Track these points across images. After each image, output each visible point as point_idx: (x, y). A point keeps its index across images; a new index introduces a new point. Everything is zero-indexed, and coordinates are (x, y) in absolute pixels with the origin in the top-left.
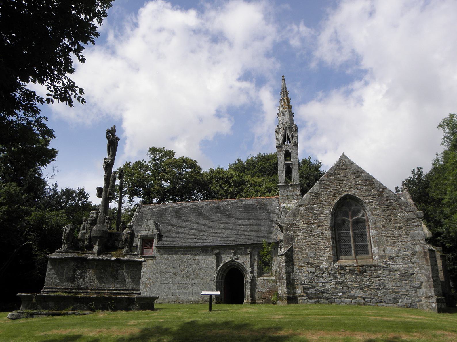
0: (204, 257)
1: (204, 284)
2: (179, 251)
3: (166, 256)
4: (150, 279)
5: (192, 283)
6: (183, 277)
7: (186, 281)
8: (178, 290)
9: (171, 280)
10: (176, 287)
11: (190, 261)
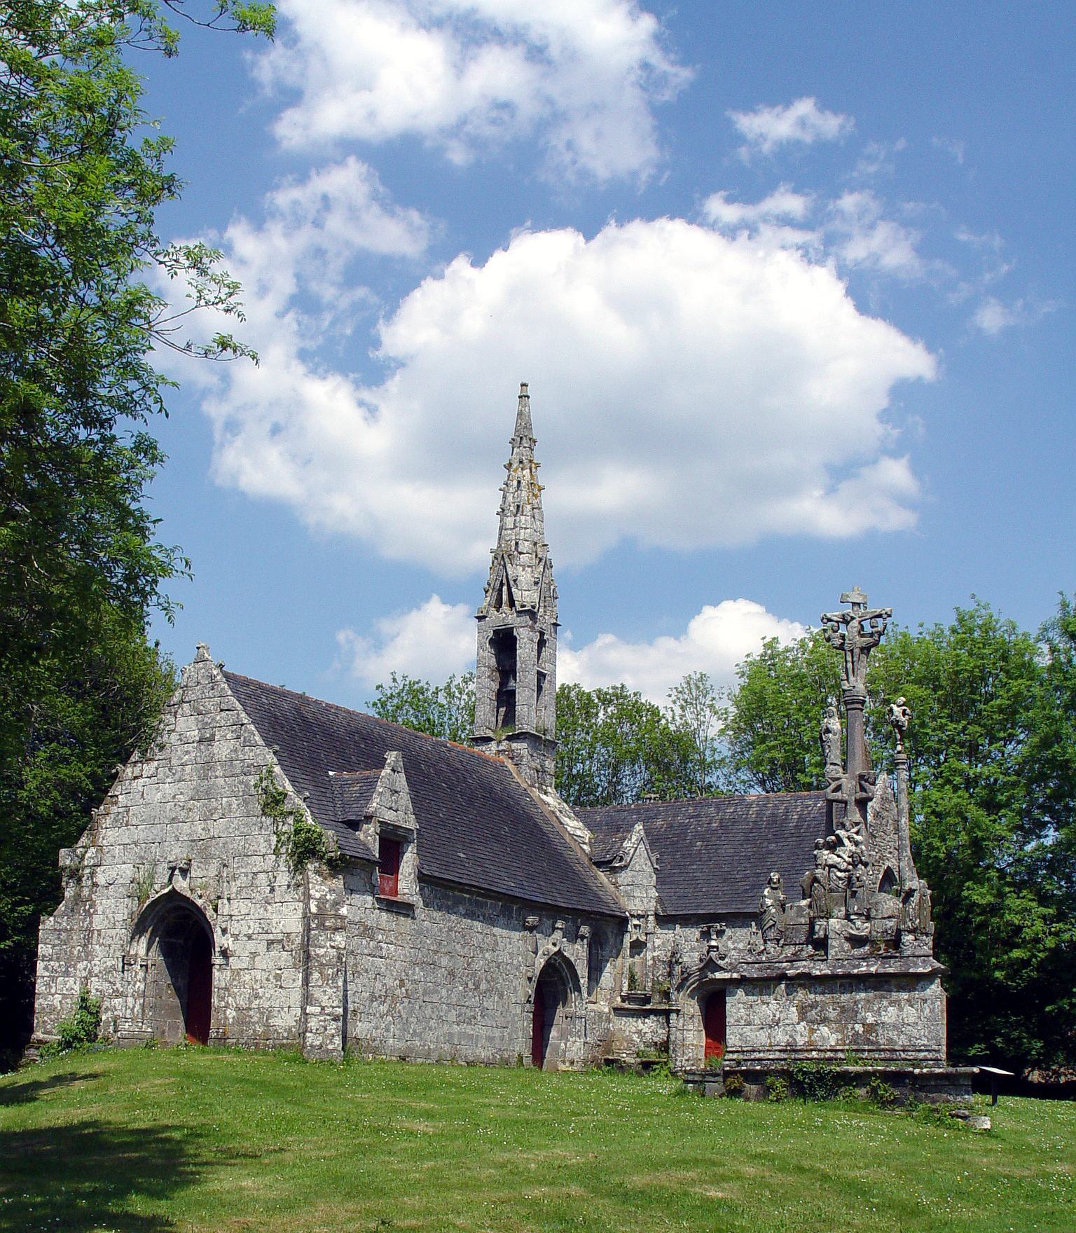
0: (505, 932)
1: (504, 1013)
2: (458, 902)
3: (437, 915)
4: (402, 985)
5: (483, 1008)
6: (467, 984)
7: (475, 1001)
8: (458, 1025)
9: (444, 992)
10: (453, 1016)
11: (480, 937)
